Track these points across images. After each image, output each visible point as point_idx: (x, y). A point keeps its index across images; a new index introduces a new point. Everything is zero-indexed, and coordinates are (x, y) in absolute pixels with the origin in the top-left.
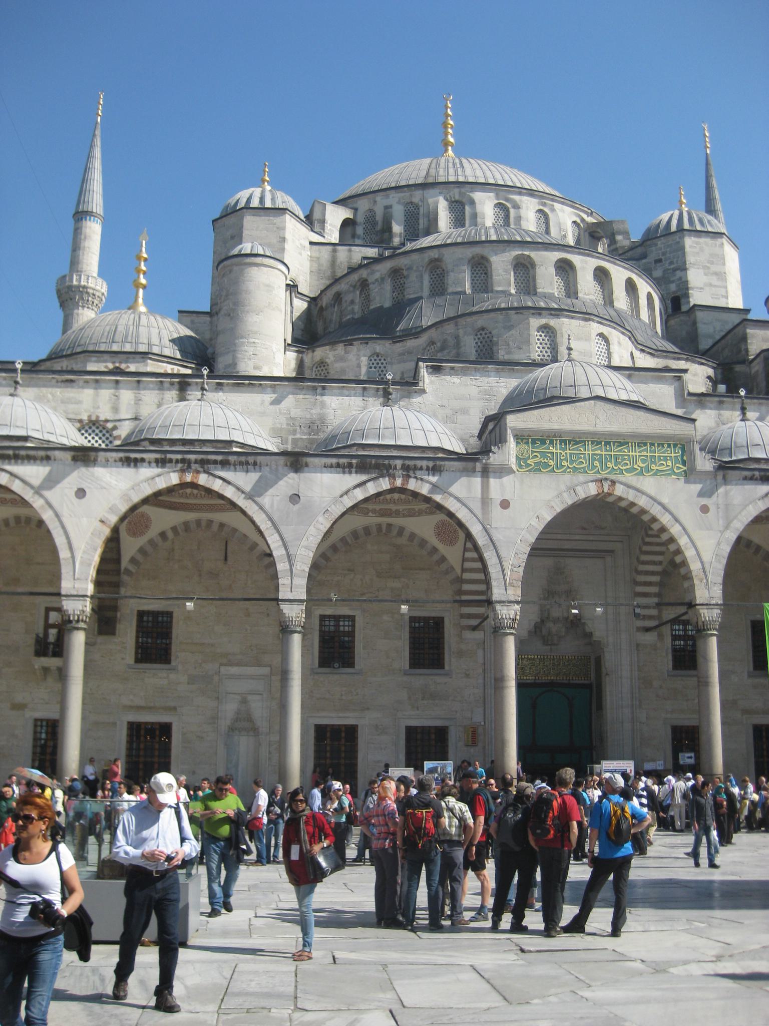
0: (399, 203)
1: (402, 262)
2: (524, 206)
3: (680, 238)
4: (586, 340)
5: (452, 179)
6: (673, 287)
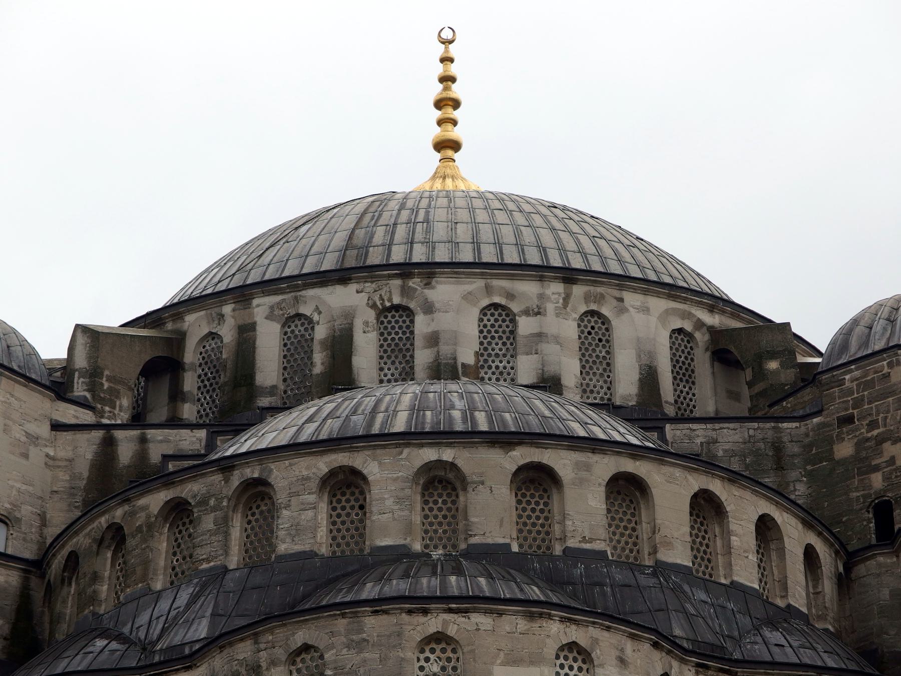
0: (270, 317)
1: (191, 490)
2: (550, 307)
3: (890, 365)
4: (532, 663)
5: (398, 255)
6: (877, 480)
